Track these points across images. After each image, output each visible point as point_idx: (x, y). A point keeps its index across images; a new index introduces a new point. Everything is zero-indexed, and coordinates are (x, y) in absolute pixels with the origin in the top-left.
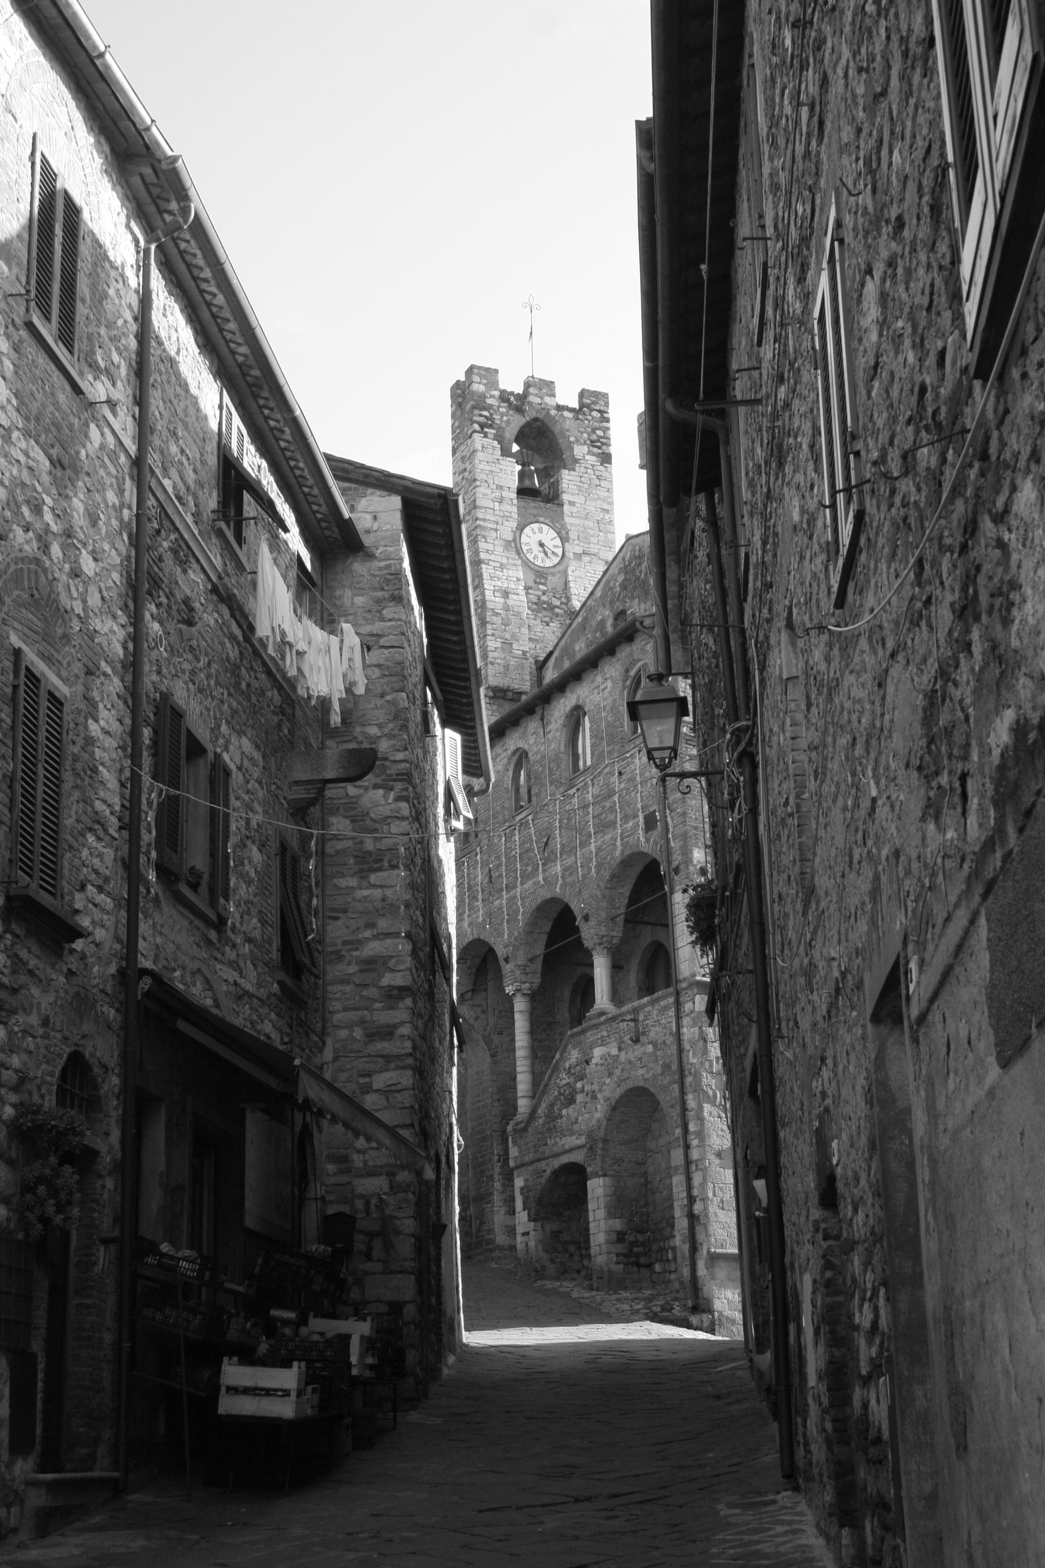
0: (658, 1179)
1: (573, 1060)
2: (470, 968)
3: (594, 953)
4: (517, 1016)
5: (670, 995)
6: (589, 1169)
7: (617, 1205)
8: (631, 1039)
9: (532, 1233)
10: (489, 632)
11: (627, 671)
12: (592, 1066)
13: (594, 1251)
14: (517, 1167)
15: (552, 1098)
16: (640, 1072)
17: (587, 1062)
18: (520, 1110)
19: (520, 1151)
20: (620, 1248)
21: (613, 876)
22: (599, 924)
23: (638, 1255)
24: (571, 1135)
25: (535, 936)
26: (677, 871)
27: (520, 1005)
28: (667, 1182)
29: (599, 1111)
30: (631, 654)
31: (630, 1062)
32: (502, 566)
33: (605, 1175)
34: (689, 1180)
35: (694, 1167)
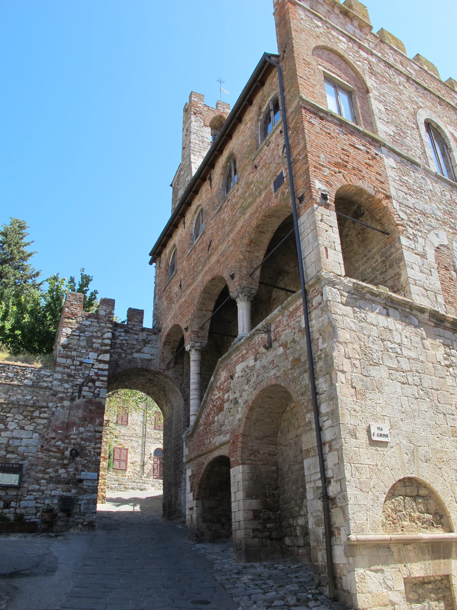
0: (287, 467)
1: (222, 379)
2: (173, 348)
3: (238, 300)
4: (192, 364)
5: (299, 297)
6: (232, 460)
8: (265, 347)
9: (195, 508)
11: (260, 108)
12: (235, 379)
13: (235, 525)
14: (188, 462)
16: (273, 372)
17: (232, 377)
19: (189, 450)
20: (255, 524)
21: (251, 241)
22: (241, 278)
23: (270, 530)
24: (220, 435)
25: (204, 312)
26: (301, 199)
27: (194, 356)
28: (296, 467)
29: (240, 413)
31: (264, 367)
33: (243, 464)
34: (323, 461)
35: (326, 449)
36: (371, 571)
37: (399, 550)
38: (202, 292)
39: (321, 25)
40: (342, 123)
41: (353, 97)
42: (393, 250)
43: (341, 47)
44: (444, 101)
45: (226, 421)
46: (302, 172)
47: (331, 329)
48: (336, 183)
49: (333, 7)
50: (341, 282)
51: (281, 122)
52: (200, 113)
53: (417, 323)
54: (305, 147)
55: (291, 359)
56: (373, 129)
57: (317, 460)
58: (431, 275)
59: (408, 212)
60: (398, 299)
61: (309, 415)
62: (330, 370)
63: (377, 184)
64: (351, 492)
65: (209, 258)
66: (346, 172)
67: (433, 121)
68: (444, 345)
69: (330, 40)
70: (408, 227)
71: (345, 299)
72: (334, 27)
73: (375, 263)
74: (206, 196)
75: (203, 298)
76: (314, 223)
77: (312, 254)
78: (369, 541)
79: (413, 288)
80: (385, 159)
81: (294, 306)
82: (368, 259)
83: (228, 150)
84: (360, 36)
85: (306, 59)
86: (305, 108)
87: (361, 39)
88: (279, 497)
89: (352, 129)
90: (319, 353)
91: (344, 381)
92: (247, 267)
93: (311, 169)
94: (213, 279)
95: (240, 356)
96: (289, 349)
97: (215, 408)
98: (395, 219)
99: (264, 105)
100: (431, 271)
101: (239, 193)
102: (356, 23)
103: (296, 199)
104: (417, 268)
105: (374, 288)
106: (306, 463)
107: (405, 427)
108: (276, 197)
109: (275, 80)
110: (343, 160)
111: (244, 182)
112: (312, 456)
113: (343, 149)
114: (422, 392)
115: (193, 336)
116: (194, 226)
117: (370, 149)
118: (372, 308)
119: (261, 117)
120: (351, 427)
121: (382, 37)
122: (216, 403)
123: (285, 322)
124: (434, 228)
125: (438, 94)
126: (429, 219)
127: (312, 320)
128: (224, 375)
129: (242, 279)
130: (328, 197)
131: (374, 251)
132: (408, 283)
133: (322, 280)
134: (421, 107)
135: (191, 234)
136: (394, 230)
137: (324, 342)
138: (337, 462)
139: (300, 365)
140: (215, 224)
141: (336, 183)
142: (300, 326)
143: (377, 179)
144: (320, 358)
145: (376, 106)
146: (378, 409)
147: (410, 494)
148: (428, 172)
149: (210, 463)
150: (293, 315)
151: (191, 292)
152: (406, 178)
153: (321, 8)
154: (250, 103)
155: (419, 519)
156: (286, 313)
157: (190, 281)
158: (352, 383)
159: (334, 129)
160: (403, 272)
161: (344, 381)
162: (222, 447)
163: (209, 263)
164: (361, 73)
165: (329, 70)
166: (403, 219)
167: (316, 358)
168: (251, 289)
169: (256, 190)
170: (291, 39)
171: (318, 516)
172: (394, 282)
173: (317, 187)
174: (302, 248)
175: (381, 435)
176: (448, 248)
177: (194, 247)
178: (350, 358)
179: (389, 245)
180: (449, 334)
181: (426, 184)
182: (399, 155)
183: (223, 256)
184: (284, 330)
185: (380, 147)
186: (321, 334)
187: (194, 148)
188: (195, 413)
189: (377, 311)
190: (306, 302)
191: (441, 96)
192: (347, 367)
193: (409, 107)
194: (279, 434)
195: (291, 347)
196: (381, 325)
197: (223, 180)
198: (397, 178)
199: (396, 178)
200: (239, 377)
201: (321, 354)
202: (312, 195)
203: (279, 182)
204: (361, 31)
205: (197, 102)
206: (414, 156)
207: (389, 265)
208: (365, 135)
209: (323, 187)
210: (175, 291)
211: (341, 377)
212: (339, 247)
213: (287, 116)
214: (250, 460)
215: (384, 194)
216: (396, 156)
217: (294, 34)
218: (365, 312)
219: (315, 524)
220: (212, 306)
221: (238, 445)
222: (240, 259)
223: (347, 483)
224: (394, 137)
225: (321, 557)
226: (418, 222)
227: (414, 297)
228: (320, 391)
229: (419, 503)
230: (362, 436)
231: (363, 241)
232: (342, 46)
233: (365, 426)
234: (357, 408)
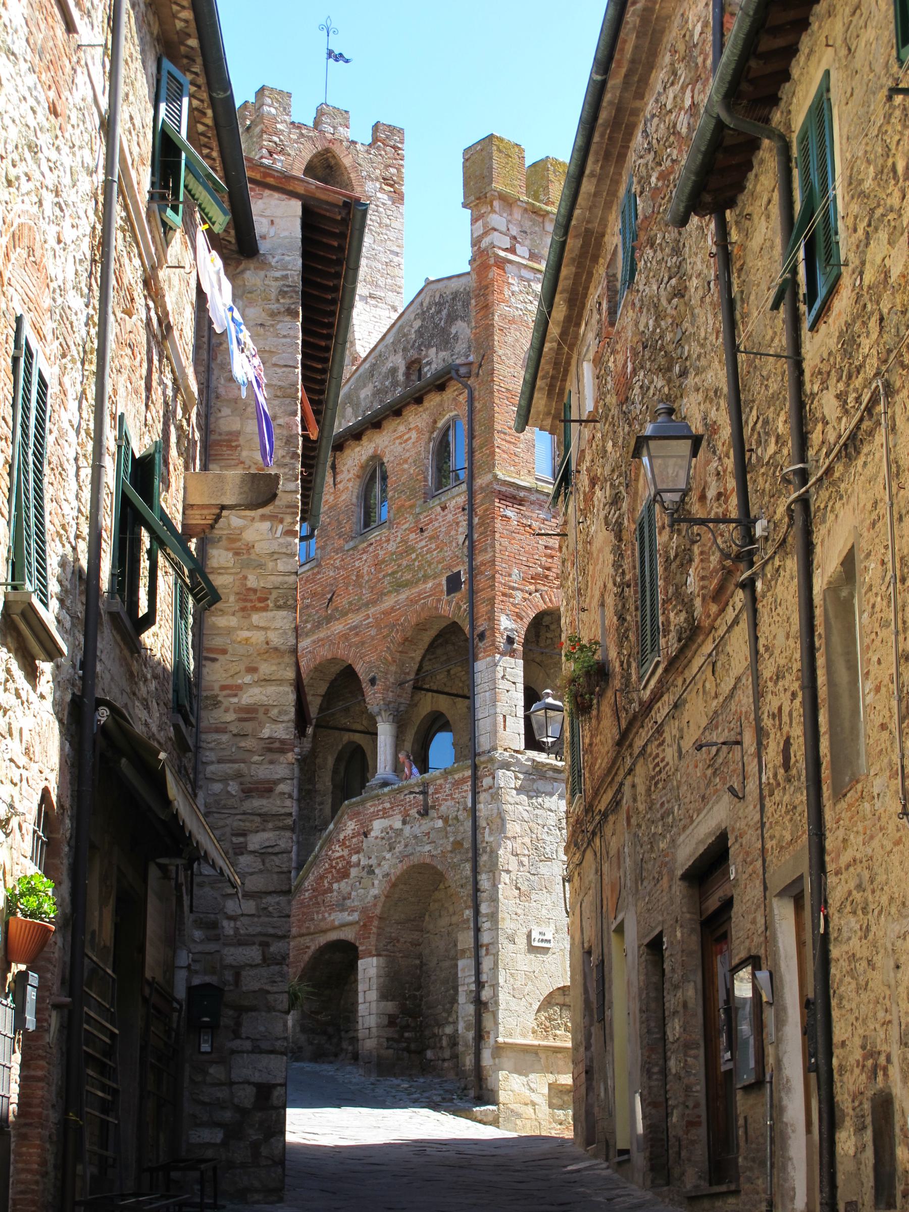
3: (379, 719)
6: (360, 948)
8: (419, 812)
11: (435, 422)
16: (428, 848)
17: (366, 835)
20: (391, 1032)
21: (406, 640)
22: (387, 689)
24: (342, 910)
26: (482, 636)
28: (447, 964)
29: (376, 888)
30: (441, 404)
31: (416, 837)
33: (378, 955)
34: (478, 964)
35: (483, 952)
37: (547, 1057)
45: (353, 893)
50: (518, 760)
52: (282, 152)
55: (451, 839)
57: (472, 962)
62: (494, 869)
64: (503, 997)
65: (329, 619)
76: (494, 680)
88: (421, 1000)
91: (507, 881)
101: (392, 547)
106: (461, 963)
108: (449, 603)
113: (546, 547)
119: (435, 435)
120: (510, 932)
137: (491, 834)
142: (465, 803)
146: (544, 911)
161: (507, 881)
163: (328, 629)
170: (491, 348)
178: (517, 855)
183: (357, 634)
184: (446, 800)
190: (475, 778)
192: (513, 865)
194: (427, 917)
195: (453, 825)
200: (377, 838)
202: (494, 641)
203: (454, 583)
205: (275, 117)
211: (505, 877)
225: (468, 1061)
228: (482, 888)
230: (522, 942)
233: (525, 931)
234: (519, 911)
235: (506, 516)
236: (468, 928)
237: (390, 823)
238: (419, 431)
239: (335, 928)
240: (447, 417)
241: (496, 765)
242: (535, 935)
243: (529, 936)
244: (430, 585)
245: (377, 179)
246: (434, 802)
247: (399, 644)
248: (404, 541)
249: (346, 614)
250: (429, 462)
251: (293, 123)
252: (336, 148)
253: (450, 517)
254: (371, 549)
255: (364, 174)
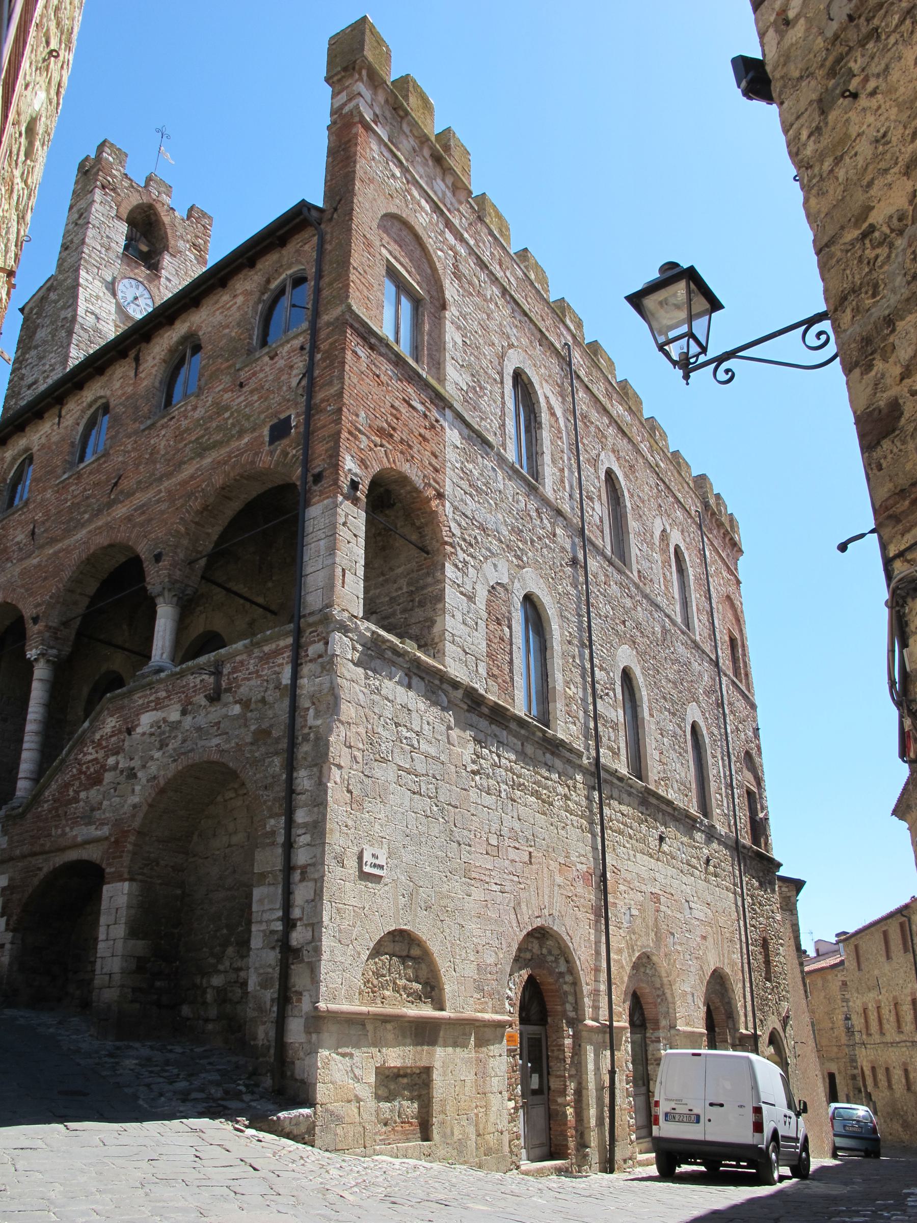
1: (108, 729)
3: (159, 600)
5: (286, 635)
6: (108, 870)
7: (147, 921)
9: (8, 946)
10: (74, 341)
11: (268, 281)
15: (67, 778)
16: (215, 741)
17: (129, 732)
18: (19, 793)
21: (205, 508)
22: (174, 565)
24: (87, 824)
26: (318, 478)
27: (41, 672)
29: (138, 795)
31: (199, 729)
32: (98, 297)
33: (131, 880)
34: (288, 893)
35: (297, 876)
36: (338, 1054)
37: (375, 1028)
38: (82, 562)
39: (399, 175)
40: (398, 361)
41: (421, 309)
42: (430, 580)
43: (422, 220)
44: (547, 338)
45: (105, 803)
46: (326, 434)
47: (330, 699)
48: (374, 463)
49: (422, 143)
51: (305, 331)
52: (114, 190)
53: (445, 704)
54: (340, 395)
56: (439, 373)
58: (476, 630)
59: (463, 523)
60: (427, 663)
61: (272, 822)
63: (429, 471)
64: (327, 942)
65: (110, 504)
66: (390, 447)
67: (526, 373)
68: (475, 740)
69: (407, 206)
70: (458, 549)
71: (358, 655)
72: (417, 182)
73: (396, 590)
74: (122, 387)
75: (81, 573)
76: (333, 526)
77: (321, 574)
78: (342, 1013)
79: (449, 648)
80: (447, 430)
81: (274, 646)
82: (386, 581)
83: (187, 324)
84: (451, 204)
85: (368, 236)
86: (352, 326)
87: (452, 209)
89: (411, 373)
90: (306, 731)
91: (338, 780)
92: (187, 548)
93: (344, 435)
94: (111, 546)
95: (152, 698)
96: (251, 711)
97: (83, 776)
98: (444, 533)
99: (275, 279)
100: (477, 623)
101: (198, 414)
102: (450, 180)
103: (309, 475)
104: (459, 616)
105: (395, 640)
106: (257, 893)
107: (407, 857)
108: (271, 453)
109: (307, 247)
110: (389, 425)
111: (210, 399)
112: (269, 884)
113: (392, 406)
114: (435, 808)
115: (47, 634)
116: (81, 429)
117: (430, 411)
118: (390, 673)
119: (265, 297)
121: (481, 209)
122: (88, 768)
123: (251, 667)
124: (493, 554)
125: (541, 325)
126: (490, 539)
127: (301, 677)
128: (113, 724)
129: (175, 567)
130: (361, 486)
131: (399, 571)
132: (442, 638)
133: (332, 622)
134: (513, 344)
135: (72, 443)
136: (438, 549)
137: (317, 716)
138: (312, 896)
139: (269, 741)
140: (134, 449)
141: (374, 463)
143: (430, 464)
144: (306, 739)
145: (452, 335)
146: (377, 826)
147: (398, 953)
148: (502, 460)
149: (55, 869)
150: (267, 658)
151: (56, 554)
152: (470, 466)
153: (405, 142)
154: (251, 263)
155: (405, 988)
156: (257, 653)
157: (59, 532)
158: (348, 784)
159: (386, 368)
160: (438, 619)
161: (338, 780)
162: (87, 846)
163: (109, 514)
164: (441, 272)
165: (395, 258)
166: (454, 535)
167: (300, 738)
168: (187, 586)
169: (233, 425)
171: (268, 973)
172: (421, 630)
173: (347, 468)
174: (306, 558)
175: (375, 866)
176: (507, 590)
177: (78, 472)
178: (350, 747)
179: (425, 571)
180: (483, 724)
181: (496, 481)
182: (468, 425)
183: (143, 513)
184: (249, 679)
185: (444, 409)
186: (313, 704)
187: (90, 256)
188: (29, 775)
189: (397, 679)
191: (544, 330)
193: (496, 342)
194: (195, 838)
195: (256, 709)
196: (399, 701)
197: (164, 371)
198: (458, 465)
199: (457, 465)
200: (144, 734)
201: (309, 734)
202: (338, 479)
203: (280, 430)
204: (454, 195)
205: (111, 164)
206: (488, 430)
207: (420, 602)
208: (427, 386)
209: (356, 470)
210: (17, 539)
211: (335, 773)
212: (361, 572)
213: (318, 326)
214: (143, 874)
215: (436, 490)
216: (463, 427)
217: (358, 184)
218: (380, 678)
219: (260, 985)
220: (92, 587)
221: (125, 847)
222: (177, 531)
223: (324, 930)
224: (467, 393)
225: (264, 1033)
226: (473, 541)
227: (448, 660)
229: (409, 967)
230: (351, 863)
231: (383, 549)
232: (422, 218)
233: (356, 850)
234: (350, 823)
235: (356, 353)
236: (273, 844)
237: (164, 715)
238: (246, 293)
239: (75, 846)
240: (284, 276)
241: (332, 625)
242: (367, 857)
243: (360, 857)
244: (246, 440)
245: (188, 242)
246: (230, 683)
247: (200, 513)
248: (216, 404)
249: (133, 494)
250: (256, 321)
251: (126, 174)
252: (158, 206)
253: (281, 363)
254: (172, 423)
255: (178, 233)
